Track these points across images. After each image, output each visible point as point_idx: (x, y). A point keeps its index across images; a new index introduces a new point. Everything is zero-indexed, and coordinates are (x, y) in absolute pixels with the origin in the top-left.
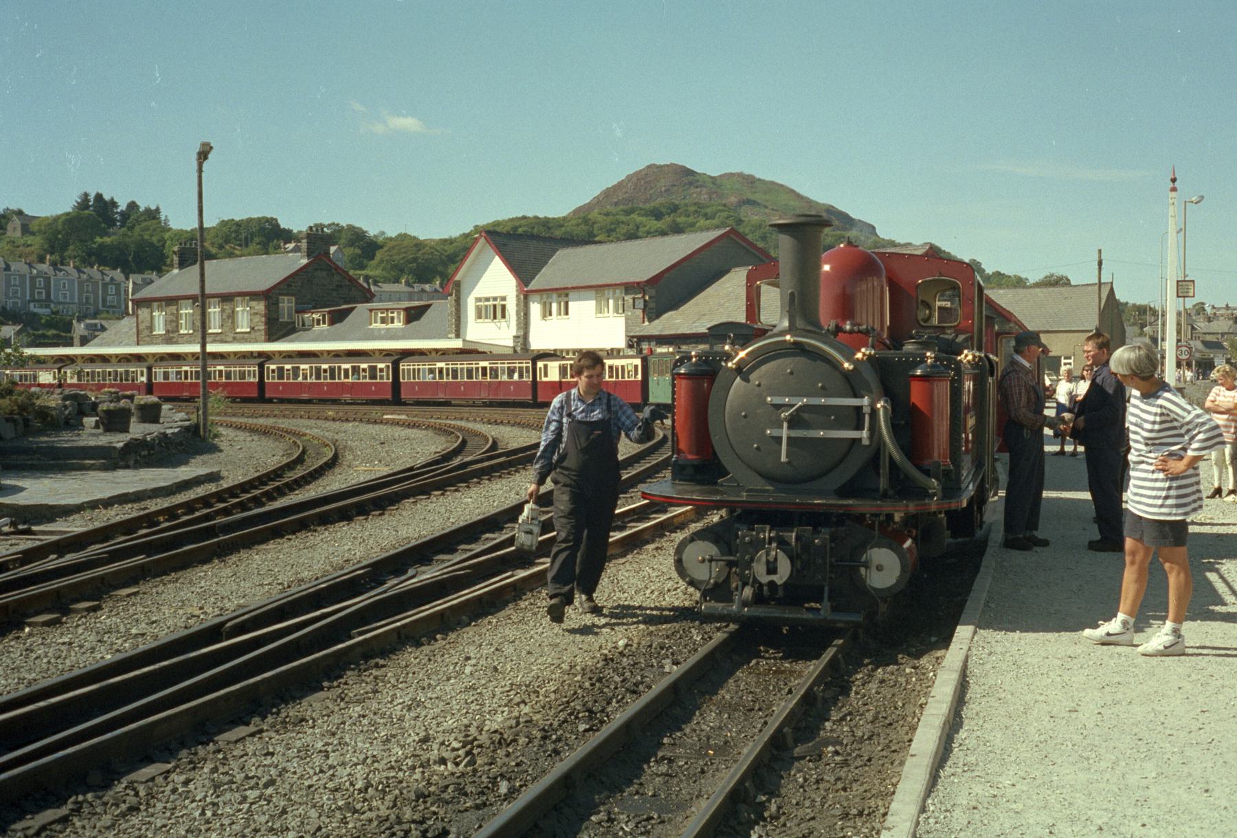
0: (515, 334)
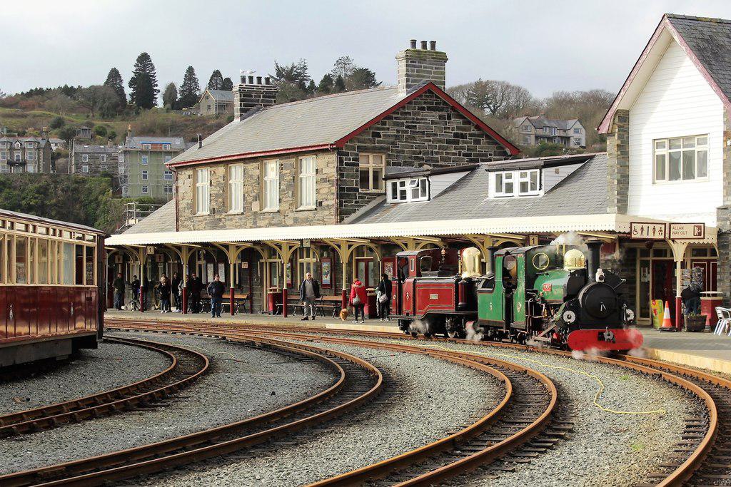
0: (721, 204)
